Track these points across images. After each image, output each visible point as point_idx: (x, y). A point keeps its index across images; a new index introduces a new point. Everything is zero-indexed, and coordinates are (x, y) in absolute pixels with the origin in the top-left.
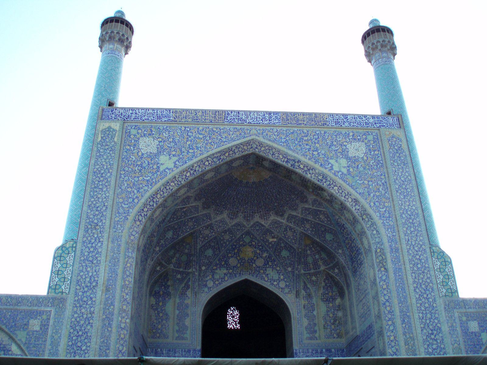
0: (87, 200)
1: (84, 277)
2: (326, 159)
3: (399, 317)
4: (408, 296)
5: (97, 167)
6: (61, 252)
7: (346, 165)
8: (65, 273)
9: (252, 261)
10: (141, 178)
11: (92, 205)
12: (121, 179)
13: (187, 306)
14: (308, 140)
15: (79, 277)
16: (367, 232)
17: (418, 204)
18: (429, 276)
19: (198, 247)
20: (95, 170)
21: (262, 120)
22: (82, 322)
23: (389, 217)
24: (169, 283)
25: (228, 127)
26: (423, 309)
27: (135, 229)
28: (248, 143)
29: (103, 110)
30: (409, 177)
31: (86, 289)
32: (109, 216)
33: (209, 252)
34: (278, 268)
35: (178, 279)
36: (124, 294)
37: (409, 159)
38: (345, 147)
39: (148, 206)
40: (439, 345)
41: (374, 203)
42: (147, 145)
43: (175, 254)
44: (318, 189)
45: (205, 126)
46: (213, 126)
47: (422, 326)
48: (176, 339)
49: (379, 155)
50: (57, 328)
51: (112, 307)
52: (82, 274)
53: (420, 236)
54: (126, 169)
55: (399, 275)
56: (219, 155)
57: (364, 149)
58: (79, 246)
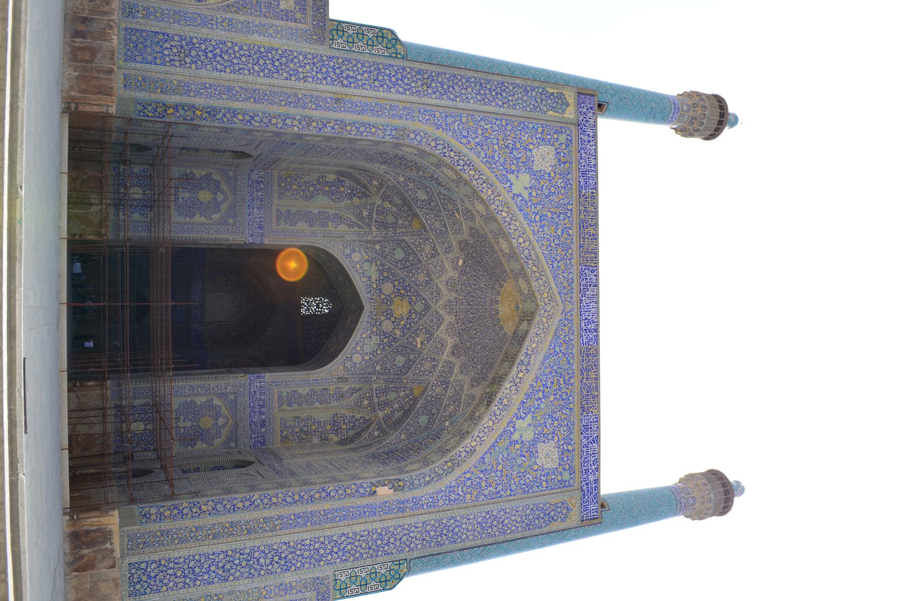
0: (462, 73)
1: (355, 68)
2: (533, 409)
3: (304, 510)
4: (335, 525)
5: (511, 88)
6: (389, 37)
7: (524, 439)
8: (360, 44)
9: (389, 315)
10: (496, 147)
11: (456, 81)
12: (494, 121)
13: (324, 225)
14: (559, 384)
16: (428, 468)
17: (468, 544)
18: (365, 556)
19: (405, 238)
20: (506, 85)
22: (292, 66)
23: (450, 500)
24: (355, 199)
25: (575, 269)
26: (317, 546)
27: (425, 140)
28: (552, 299)
29: (593, 95)
30: (509, 532)
31: (338, 71)
32: (442, 103)
33: (400, 254)
34: (379, 352)
35: (361, 213)
36: (332, 124)
37: (537, 531)
38: (550, 437)
39: (457, 158)
40: (265, 568)
42: (544, 157)
43: (396, 205)
44: (489, 399)
46: (575, 249)
47: (292, 544)
48: (277, 210)
49: (540, 488)
50: (284, 33)
51: (314, 107)
53: (423, 545)
54: (509, 128)
55: (365, 513)
56: (534, 257)
57: (549, 466)
58: (399, 63)
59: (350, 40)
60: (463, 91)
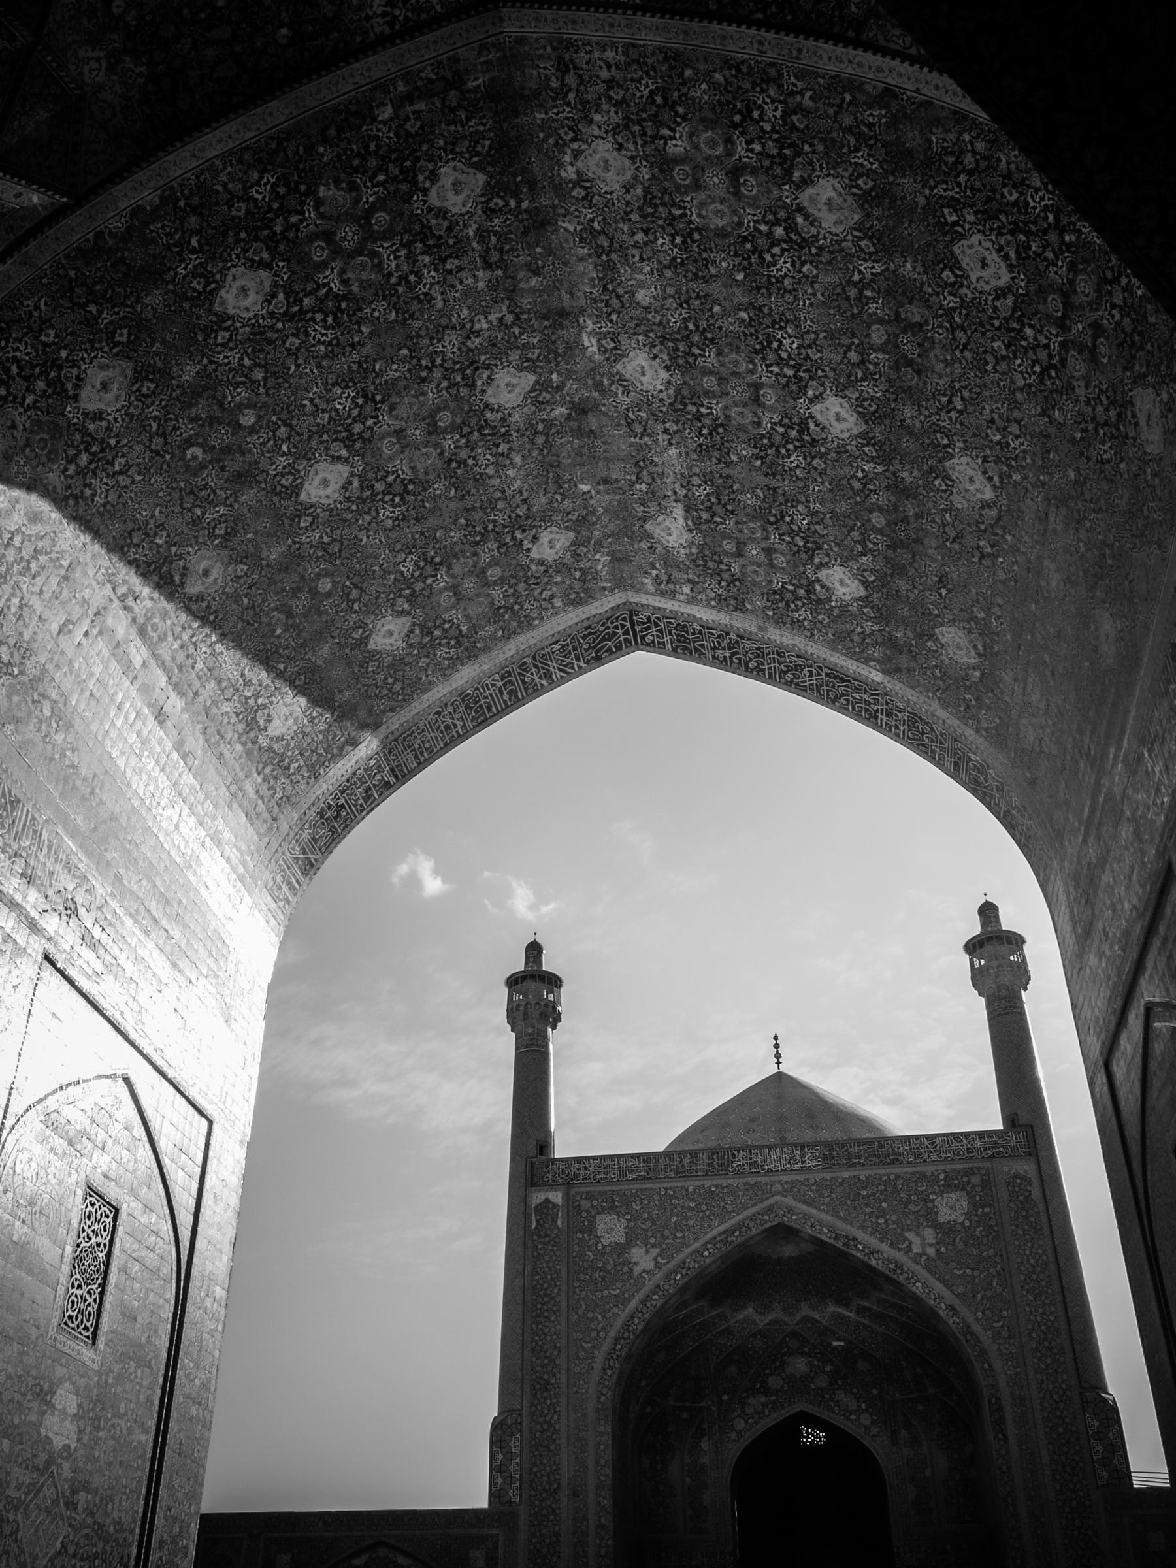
7: (934, 1241)
10: (606, 1292)
18: (1077, 1448)
22: (545, 1551)
26: (1067, 1510)
28: (769, 1210)
29: (532, 1164)
30: (1044, 1257)
31: (544, 1495)
37: (1044, 1219)
38: (930, 1205)
39: (622, 1342)
45: (697, 1183)
52: (535, 1469)
56: (724, 1236)
57: (965, 1204)
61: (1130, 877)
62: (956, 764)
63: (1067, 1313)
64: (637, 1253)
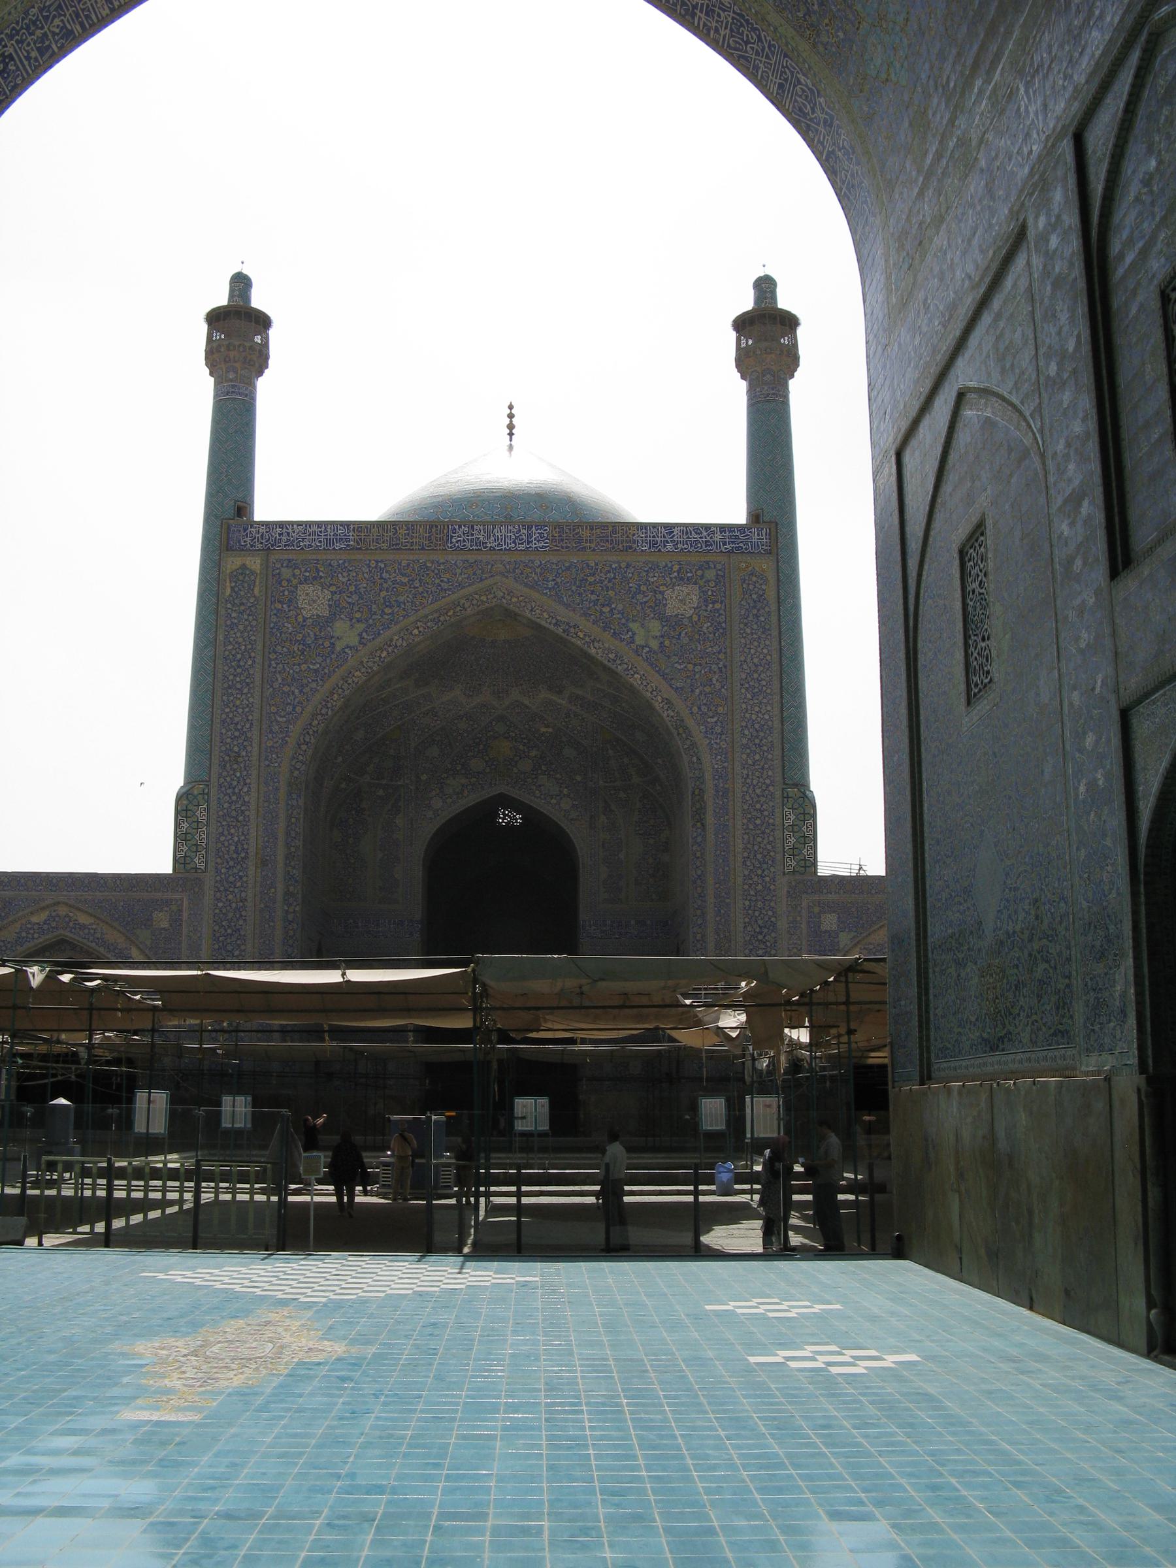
2: (623, 621)
5: (230, 647)
7: (658, 634)
10: (304, 667)
15: (219, 845)
17: (776, 712)
18: (771, 839)
21: (514, 542)
23: (722, 733)
26: (752, 893)
27: (301, 758)
29: (229, 528)
30: (769, 658)
31: (231, 863)
36: (290, 869)
37: (774, 619)
39: (319, 717)
41: (699, 708)
56: (436, 615)
58: (214, 791)
59: (194, 848)
60: (240, 710)
61: (969, 241)
62: (781, 86)
63: (782, 712)
64: (340, 627)
